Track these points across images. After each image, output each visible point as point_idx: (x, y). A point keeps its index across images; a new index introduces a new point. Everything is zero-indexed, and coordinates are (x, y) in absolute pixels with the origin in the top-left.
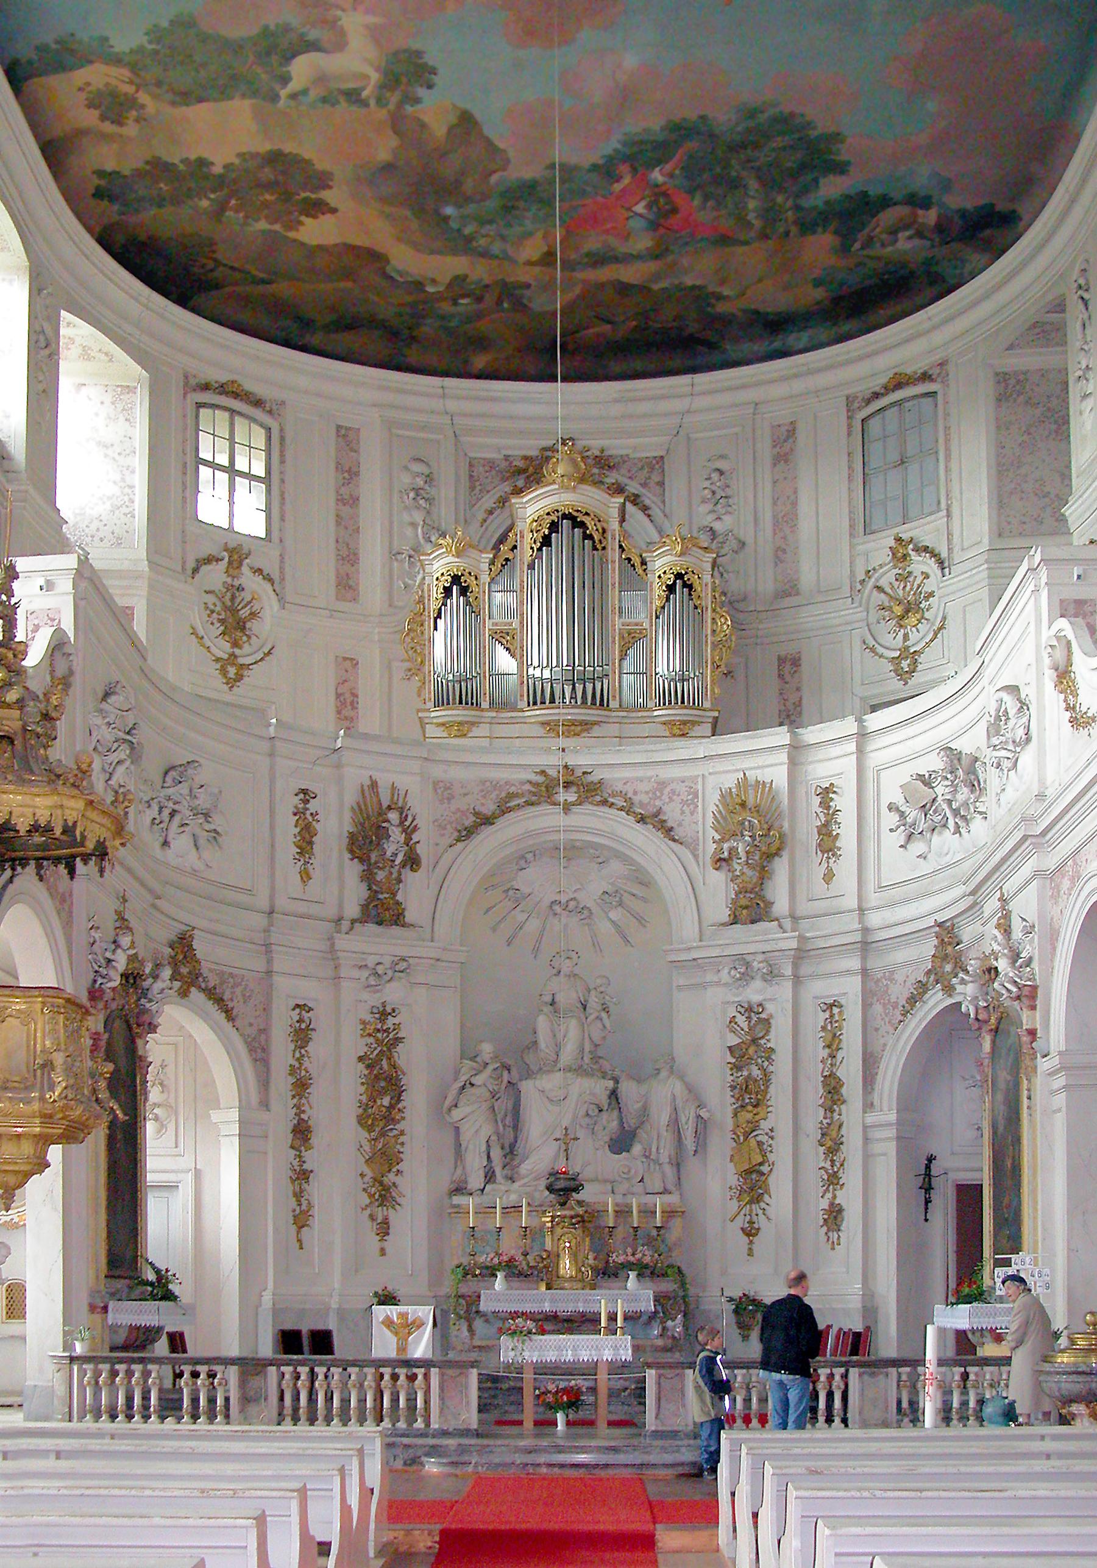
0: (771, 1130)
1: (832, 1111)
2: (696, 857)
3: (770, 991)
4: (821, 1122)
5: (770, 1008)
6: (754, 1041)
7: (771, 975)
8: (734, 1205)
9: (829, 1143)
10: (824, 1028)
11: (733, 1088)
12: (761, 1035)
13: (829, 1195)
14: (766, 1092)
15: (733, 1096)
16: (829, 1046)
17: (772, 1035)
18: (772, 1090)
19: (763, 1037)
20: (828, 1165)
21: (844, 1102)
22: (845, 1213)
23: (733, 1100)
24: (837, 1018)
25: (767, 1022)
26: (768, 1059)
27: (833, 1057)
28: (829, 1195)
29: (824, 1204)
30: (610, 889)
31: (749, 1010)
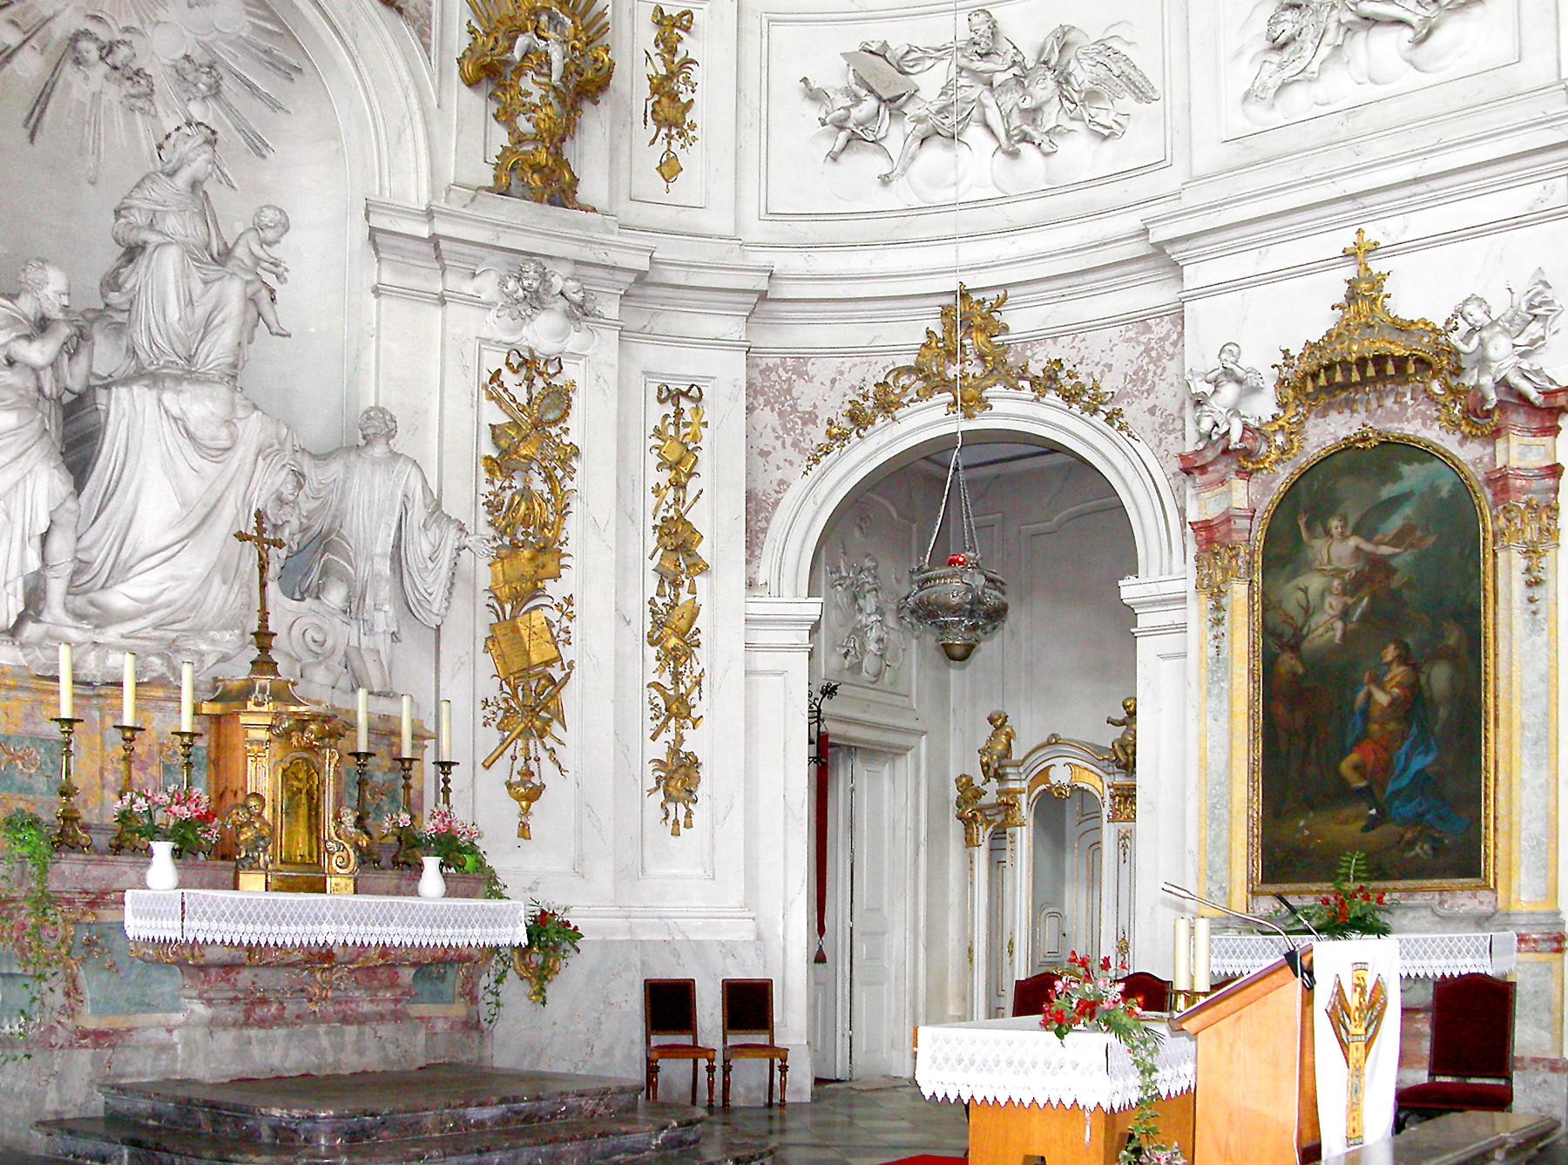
0: (569, 600)
1: (676, 585)
2: (427, 47)
3: (576, 340)
4: (652, 602)
5: (571, 371)
6: (538, 425)
7: (580, 312)
8: (493, 737)
9: (673, 641)
10: (658, 432)
11: (493, 507)
12: (551, 416)
13: (668, 736)
14: (557, 527)
15: (491, 524)
16: (674, 466)
17: (572, 422)
18: (572, 525)
19: (555, 422)
20: (666, 680)
21: (705, 569)
22: (704, 773)
23: (491, 532)
24: (687, 417)
25: (561, 399)
26: (564, 463)
27: (679, 486)
28: (668, 736)
29: (659, 750)
30: (197, 54)
31: (528, 364)
